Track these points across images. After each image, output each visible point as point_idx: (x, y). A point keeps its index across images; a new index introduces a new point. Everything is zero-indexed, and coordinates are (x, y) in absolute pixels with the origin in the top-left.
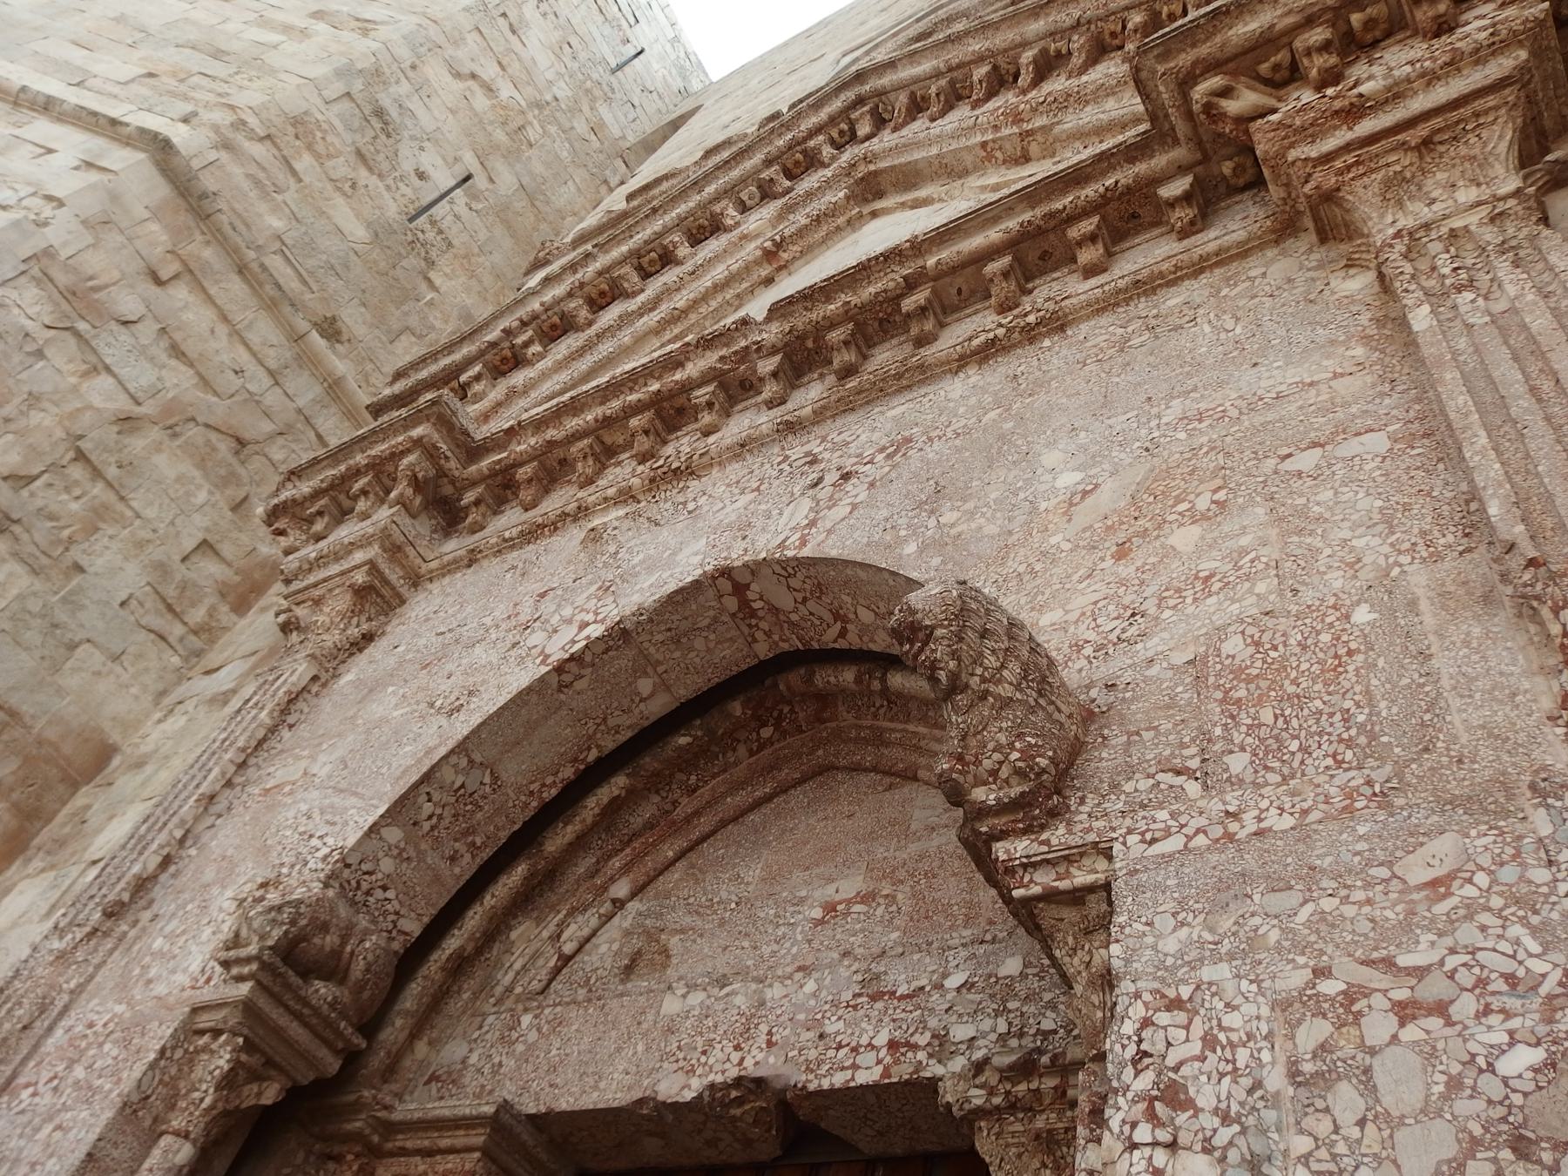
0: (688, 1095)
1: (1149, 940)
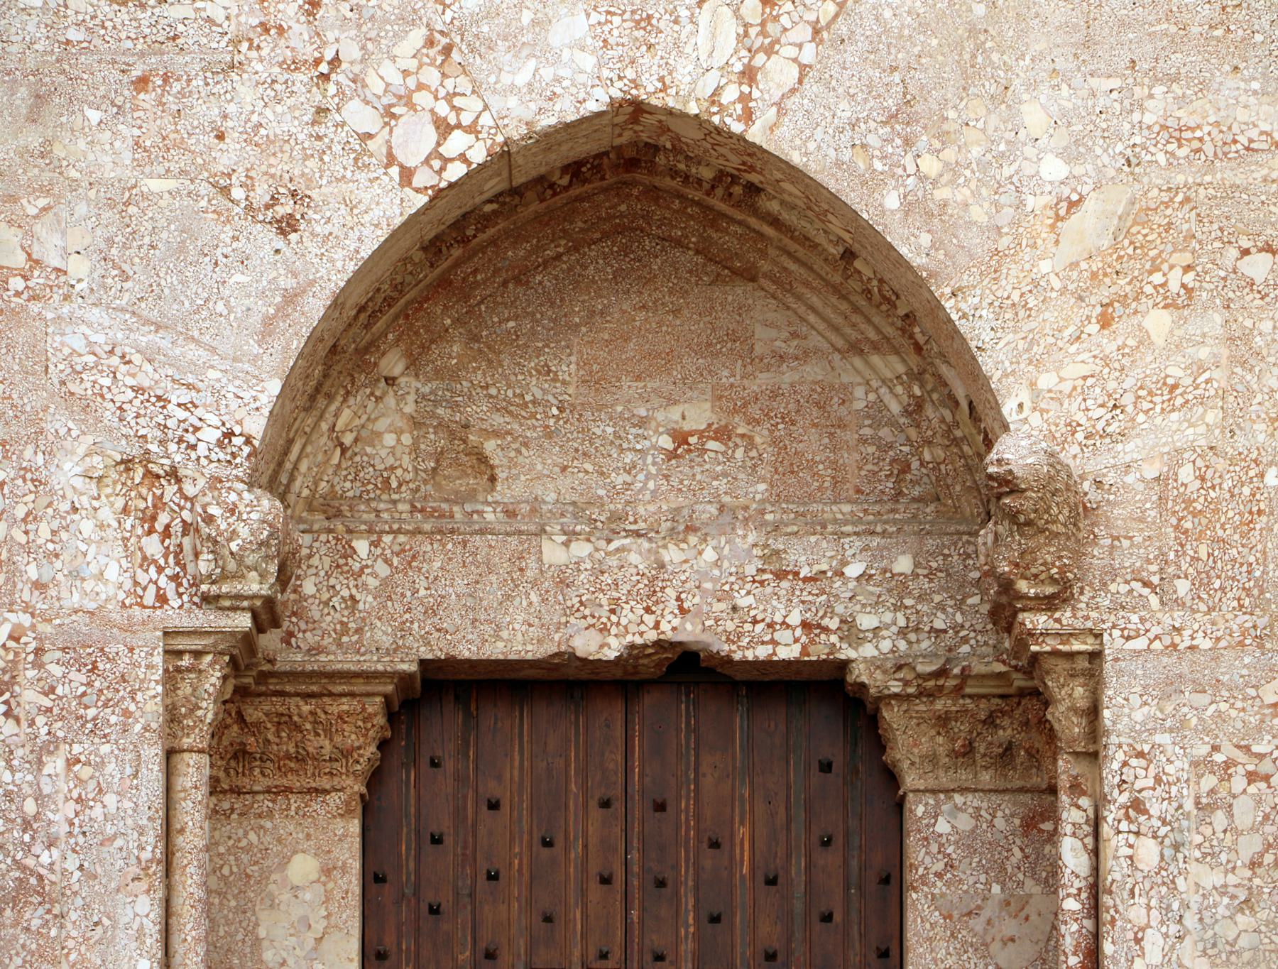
0: (611, 655)
1: (1126, 710)
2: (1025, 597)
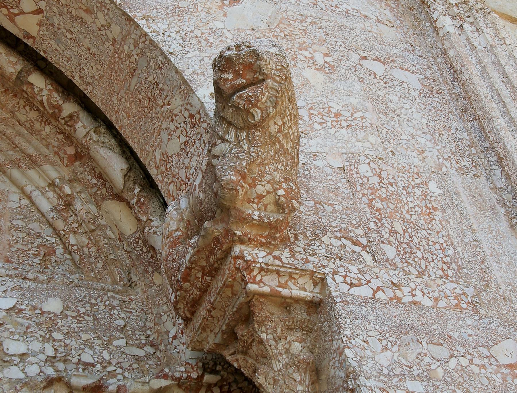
1: (368, 353)
2: (245, 220)
